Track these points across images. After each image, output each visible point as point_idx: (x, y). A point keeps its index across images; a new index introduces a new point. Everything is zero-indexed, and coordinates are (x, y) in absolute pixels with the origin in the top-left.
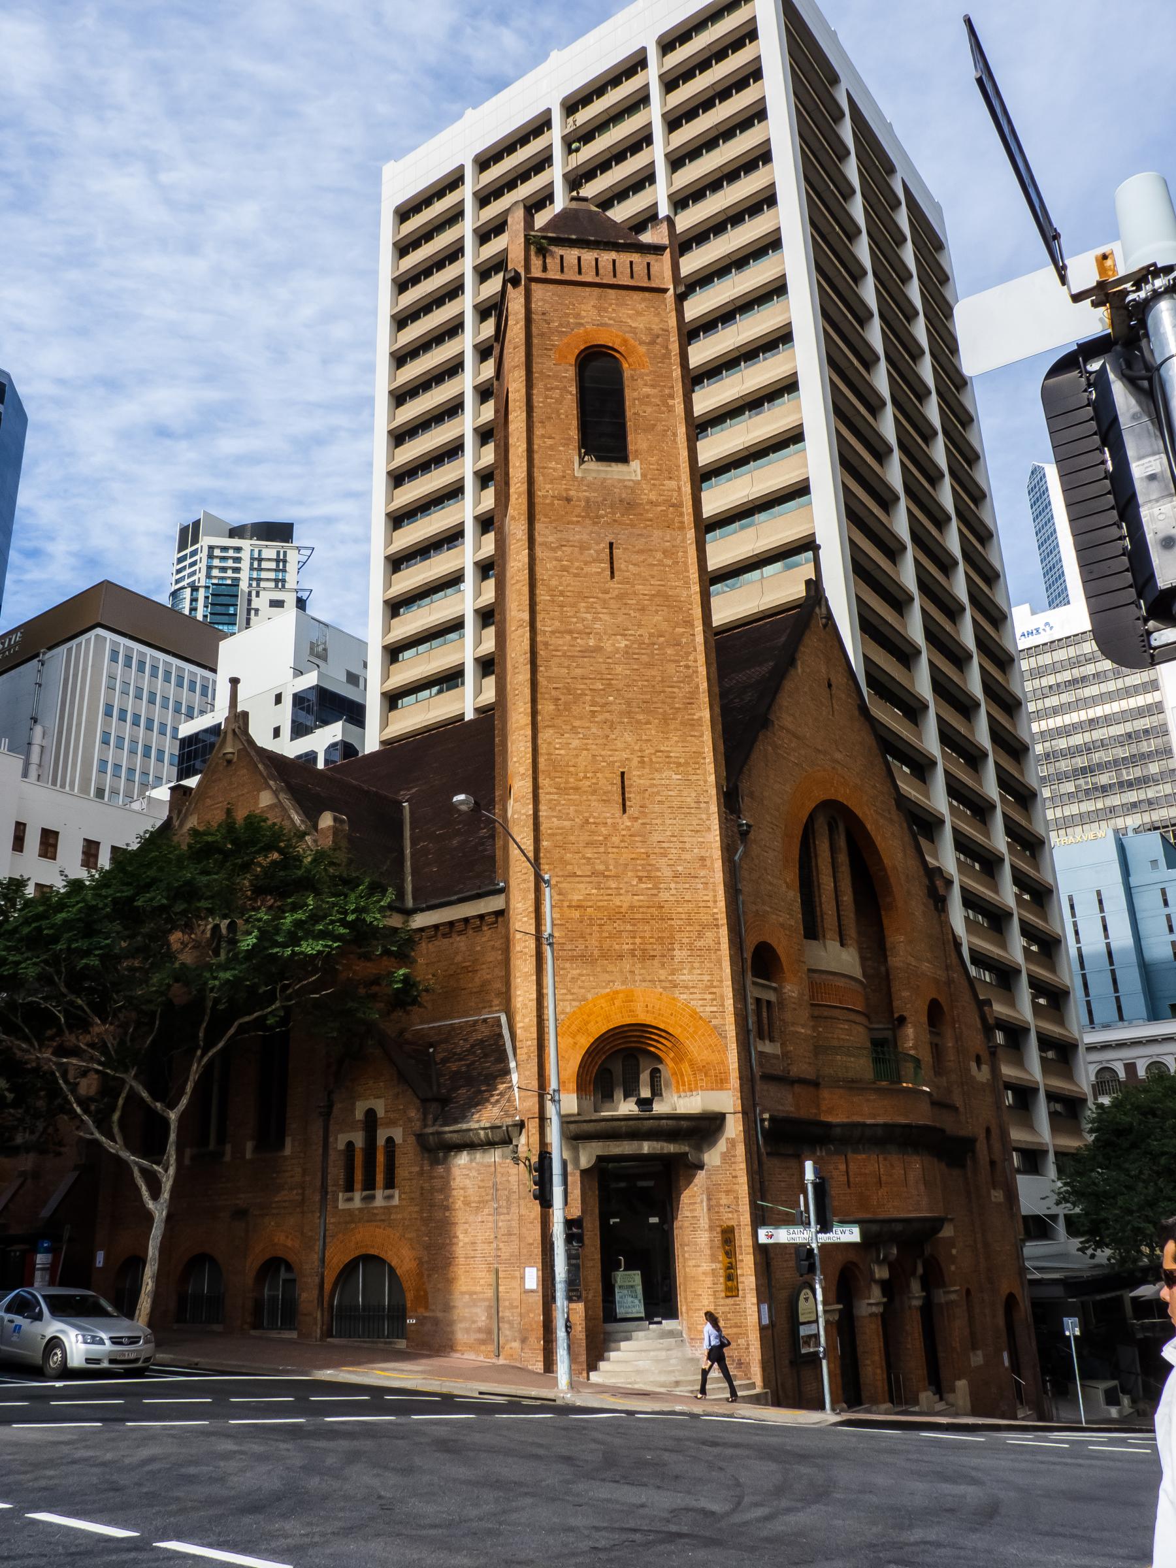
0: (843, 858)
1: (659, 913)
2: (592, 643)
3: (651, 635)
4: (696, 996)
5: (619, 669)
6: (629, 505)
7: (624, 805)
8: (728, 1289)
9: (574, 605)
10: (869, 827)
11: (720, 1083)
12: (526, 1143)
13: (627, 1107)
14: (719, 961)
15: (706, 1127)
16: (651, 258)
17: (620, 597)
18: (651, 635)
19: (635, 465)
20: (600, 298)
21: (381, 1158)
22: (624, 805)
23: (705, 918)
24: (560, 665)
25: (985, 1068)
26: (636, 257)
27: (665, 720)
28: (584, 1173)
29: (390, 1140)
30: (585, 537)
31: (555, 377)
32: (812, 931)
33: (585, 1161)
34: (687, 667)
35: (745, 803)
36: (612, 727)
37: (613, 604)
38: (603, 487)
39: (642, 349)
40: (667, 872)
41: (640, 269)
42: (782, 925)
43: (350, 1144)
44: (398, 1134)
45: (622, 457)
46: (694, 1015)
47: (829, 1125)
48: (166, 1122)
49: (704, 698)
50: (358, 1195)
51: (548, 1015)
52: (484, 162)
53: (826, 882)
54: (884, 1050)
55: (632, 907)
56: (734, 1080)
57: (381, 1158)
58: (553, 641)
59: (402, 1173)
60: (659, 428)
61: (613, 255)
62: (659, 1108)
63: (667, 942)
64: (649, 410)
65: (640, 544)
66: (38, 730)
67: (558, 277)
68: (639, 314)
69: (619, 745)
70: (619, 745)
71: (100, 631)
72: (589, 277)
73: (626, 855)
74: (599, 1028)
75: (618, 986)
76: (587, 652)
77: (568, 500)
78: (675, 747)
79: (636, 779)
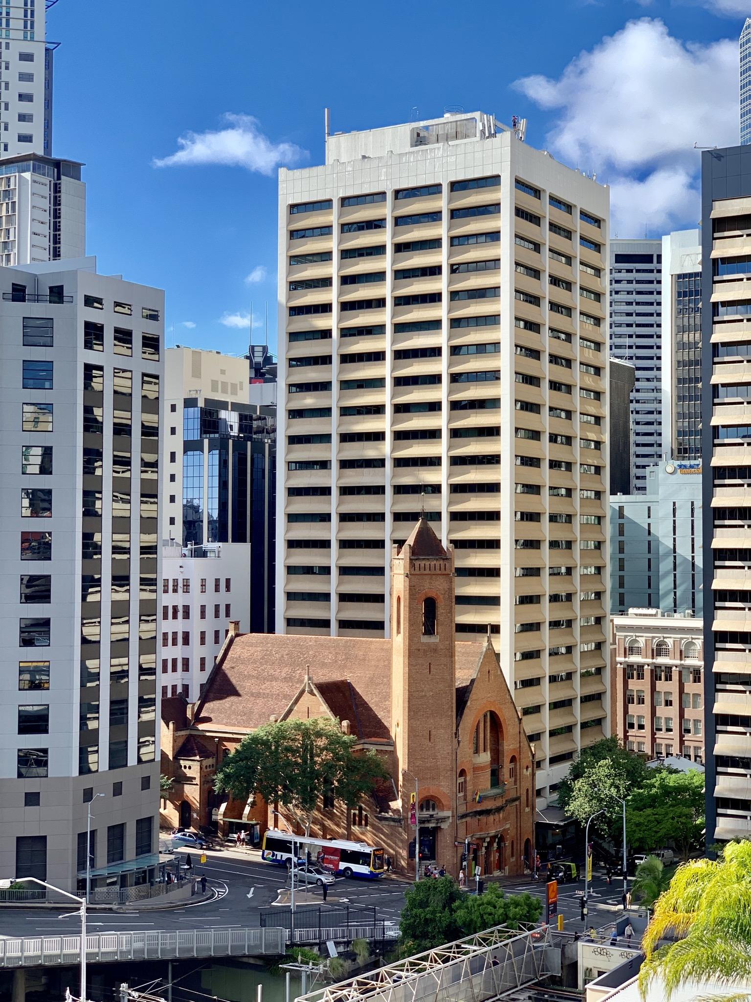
6: (435, 650)
11: (449, 809)
25: (530, 769)
26: (442, 562)
32: (477, 751)
36: (428, 718)
38: (428, 644)
53: (481, 735)
72: (427, 572)
76: (422, 697)
79: (433, 733)
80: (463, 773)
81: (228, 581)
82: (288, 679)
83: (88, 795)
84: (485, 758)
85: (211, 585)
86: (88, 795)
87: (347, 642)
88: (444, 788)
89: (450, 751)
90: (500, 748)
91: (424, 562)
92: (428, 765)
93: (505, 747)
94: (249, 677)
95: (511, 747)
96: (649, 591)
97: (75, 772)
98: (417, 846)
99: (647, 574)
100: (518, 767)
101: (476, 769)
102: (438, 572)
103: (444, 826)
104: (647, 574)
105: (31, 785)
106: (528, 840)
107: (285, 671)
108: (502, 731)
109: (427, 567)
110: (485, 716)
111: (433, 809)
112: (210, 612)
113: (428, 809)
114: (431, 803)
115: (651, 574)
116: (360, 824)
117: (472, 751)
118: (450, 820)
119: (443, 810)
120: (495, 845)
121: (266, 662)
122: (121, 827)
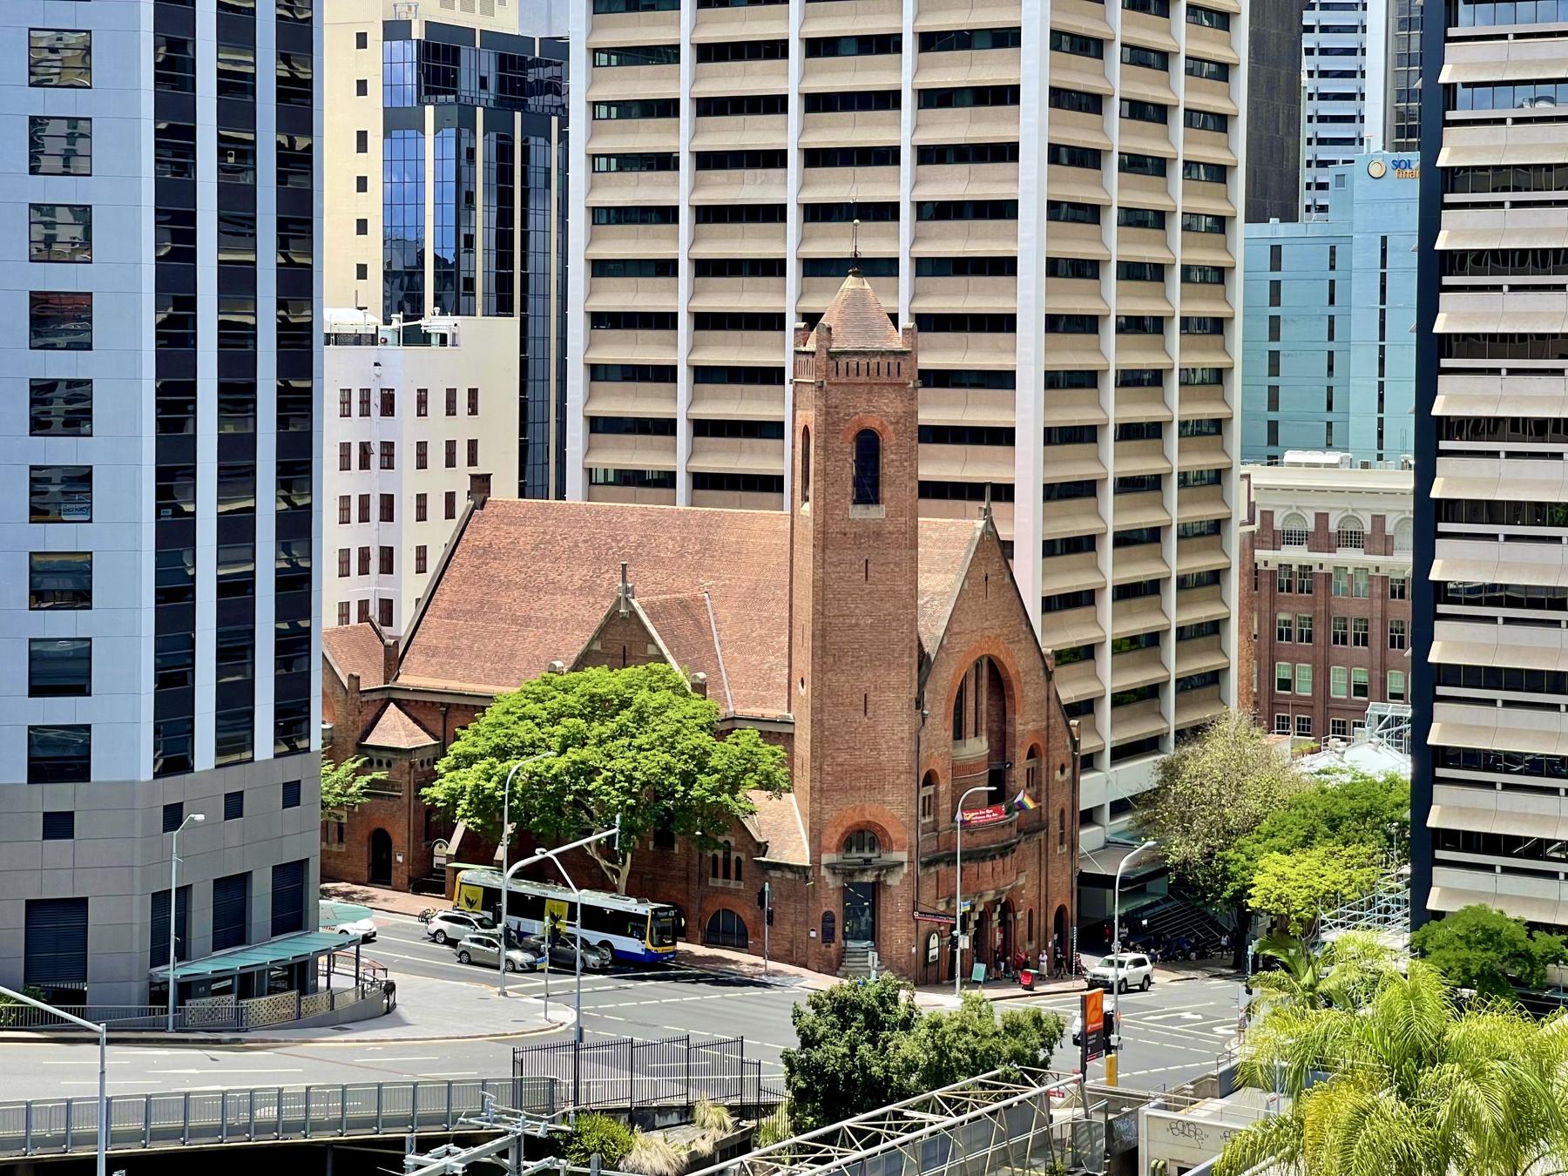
0: (984, 682)
1: (880, 767)
4: (894, 809)
6: (878, 535)
11: (902, 848)
20: (870, 392)
21: (733, 866)
25: (1068, 771)
26: (892, 360)
29: (738, 859)
31: (841, 452)
35: (928, 706)
39: (891, 428)
41: (894, 369)
43: (715, 856)
44: (743, 857)
45: (877, 502)
46: (893, 816)
50: (720, 882)
54: (998, 777)
57: (733, 866)
59: (744, 874)
63: (882, 781)
67: (844, 381)
72: (863, 378)
73: (865, 737)
76: (851, 627)
78: (893, 679)
79: (872, 698)
80: (930, 779)
81: (473, 393)
82: (588, 589)
83: (173, 816)
84: (977, 747)
85: (437, 402)
86: (173, 816)
87: (704, 516)
88: (894, 809)
89: (906, 735)
90: (1009, 729)
92: (864, 761)
93: (1019, 728)
94: (508, 585)
95: (1030, 727)
96: (1330, 417)
97: (146, 770)
98: (194, 1071)
99: (1327, 382)
100: (1044, 766)
101: (959, 769)
102: (884, 378)
103: (894, 880)
104: (1327, 382)
105: (59, 796)
106: (1061, 910)
107: (581, 573)
108: (1012, 697)
109: (863, 368)
110: (977, 666)
111: (872, 850)
112: (436, 455)
113: (861, 849)
114: (868, 835)
115: (1333, 382)
116: (727, 876)
117: (951, 733)
118: (906, 869)
119: (890, 850)
120: (995, 916)
121: (543, 556)
122: (243, 879)
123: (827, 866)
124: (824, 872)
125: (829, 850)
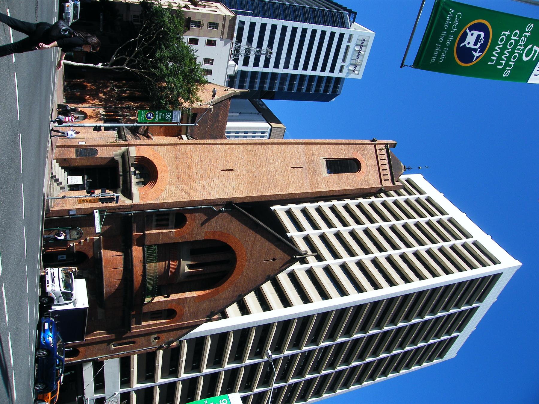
2: (271, 161)
3: (276, 179)
5: (264, 169)
6: (314, 173)
7: (223, 170)
8: (80, 200)
9: (281, 156)
10: (230, 279)
11: (141, 199)
12: (121, 142)
13: (132, 169)
14: (179, 198)
15: (128, 194)
16: (390, 180)
17: (286, 169)
18: (276, 179)
19: (328, 175)
22: (223, 170)
23: (192, 195)
24: (263, 152)
26: (389, 176)
27: (251, 183)
28: (113, 158)
30: (303, 160)
33: (116, 158)
34: (269, 190)
37: (284, 168)
39: (362, 177)
40: (204, 183)
42: (193, 229)
46: (162, 191)
47: (131, 248)
48: (123, 65)
49: (259, 194)
51: (159, 150)
52: (428, 199)
55: (193, 172)
56: (142, 203)
58: (270, 150)
60: (340, 182)
61: (389, 170)
62: (133, 177)
64: (345, 179)
65: (304, 176)
66: (238, 114)
68: (373, 177)
69: (242, 169)
70: (242, 169)
71: (270, 127)
73: (208, 171)
74: (155, 162)
75: (169, 168)
76: (268, 159)
77: (313, 155)
91: (387, 159)
118: (128, 202)
123: (127, 150)
124: (124, 148)
125: (138, 151)
